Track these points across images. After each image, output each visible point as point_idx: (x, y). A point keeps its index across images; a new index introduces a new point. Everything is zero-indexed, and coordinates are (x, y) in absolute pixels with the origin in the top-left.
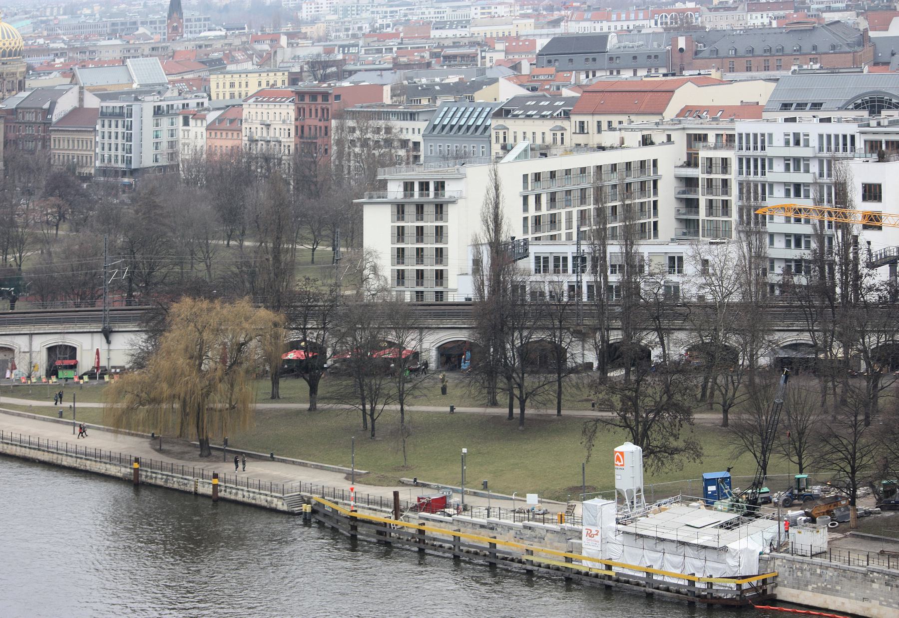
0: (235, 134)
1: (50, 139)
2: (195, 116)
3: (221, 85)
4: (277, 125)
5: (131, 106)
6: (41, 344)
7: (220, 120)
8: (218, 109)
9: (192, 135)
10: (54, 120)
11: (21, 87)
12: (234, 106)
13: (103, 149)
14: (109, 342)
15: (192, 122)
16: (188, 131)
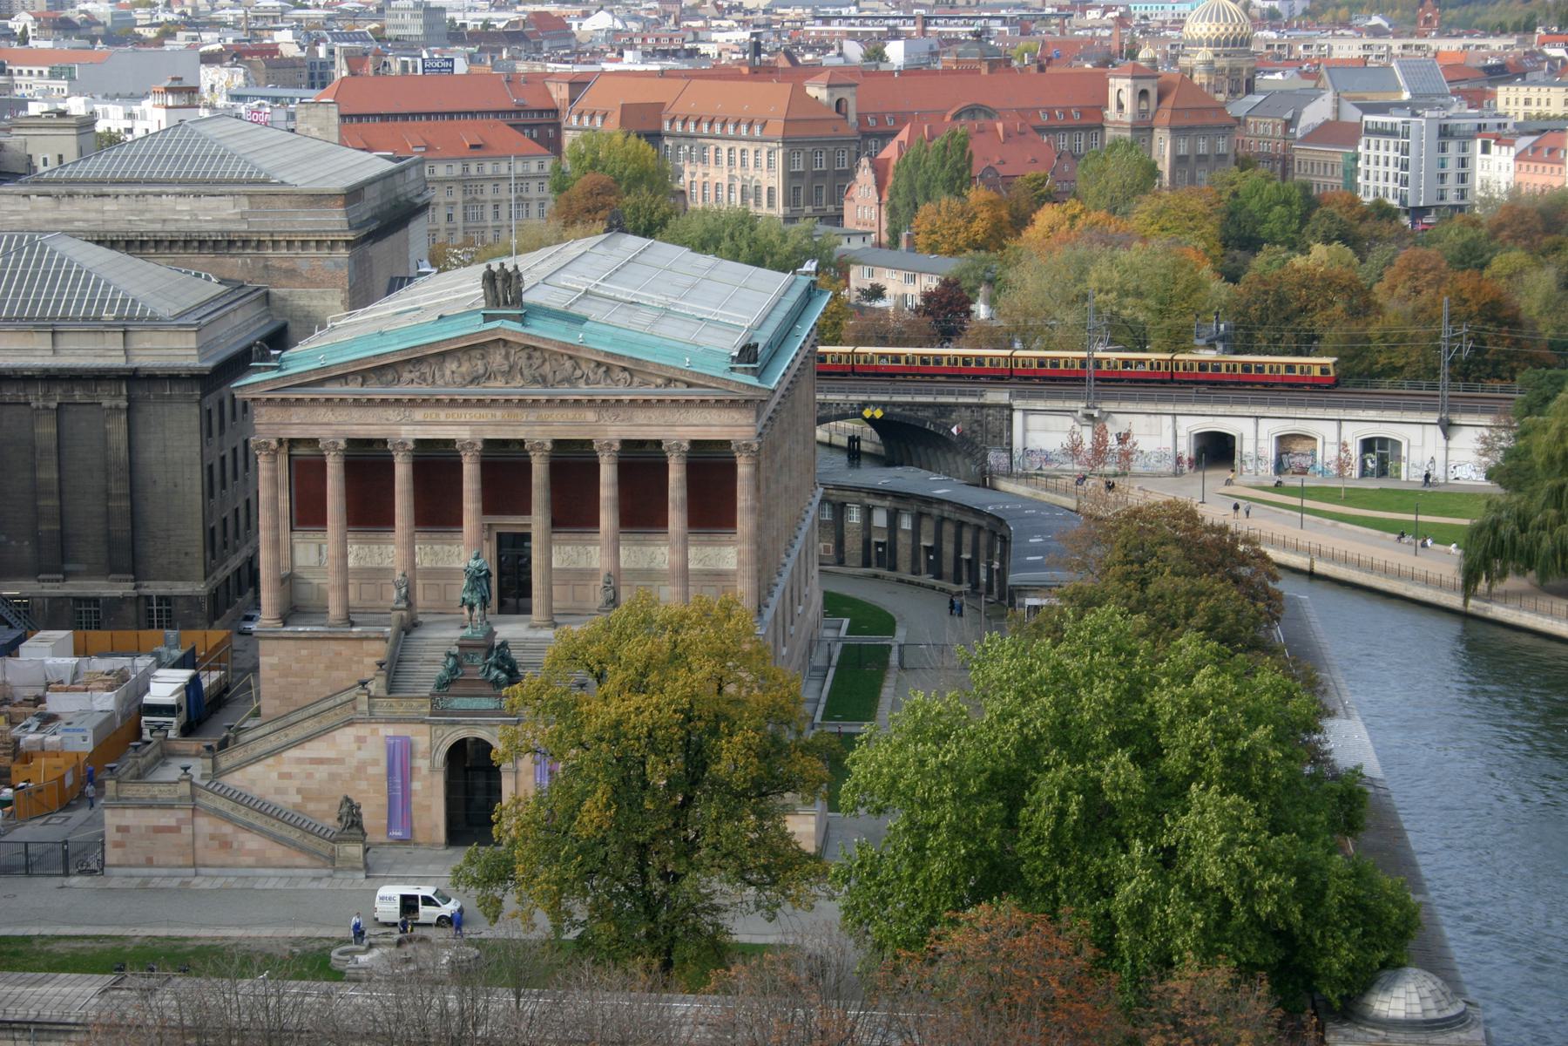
0: (1556, 167)
1: (1293, 160)
2: (1499, 141)
3: (1512, 101)
5: (1408, 122)
6: (1354, 434)
7: (1535, 148)
8: (1530, 134)
9: (1494, 165)
10: (1299, 135)
11: (1250, 89)
12: (1552, 131)
13: (1367, 178)
14: (1447, 437)
15: (1494, 149)
16: (1489, 160)
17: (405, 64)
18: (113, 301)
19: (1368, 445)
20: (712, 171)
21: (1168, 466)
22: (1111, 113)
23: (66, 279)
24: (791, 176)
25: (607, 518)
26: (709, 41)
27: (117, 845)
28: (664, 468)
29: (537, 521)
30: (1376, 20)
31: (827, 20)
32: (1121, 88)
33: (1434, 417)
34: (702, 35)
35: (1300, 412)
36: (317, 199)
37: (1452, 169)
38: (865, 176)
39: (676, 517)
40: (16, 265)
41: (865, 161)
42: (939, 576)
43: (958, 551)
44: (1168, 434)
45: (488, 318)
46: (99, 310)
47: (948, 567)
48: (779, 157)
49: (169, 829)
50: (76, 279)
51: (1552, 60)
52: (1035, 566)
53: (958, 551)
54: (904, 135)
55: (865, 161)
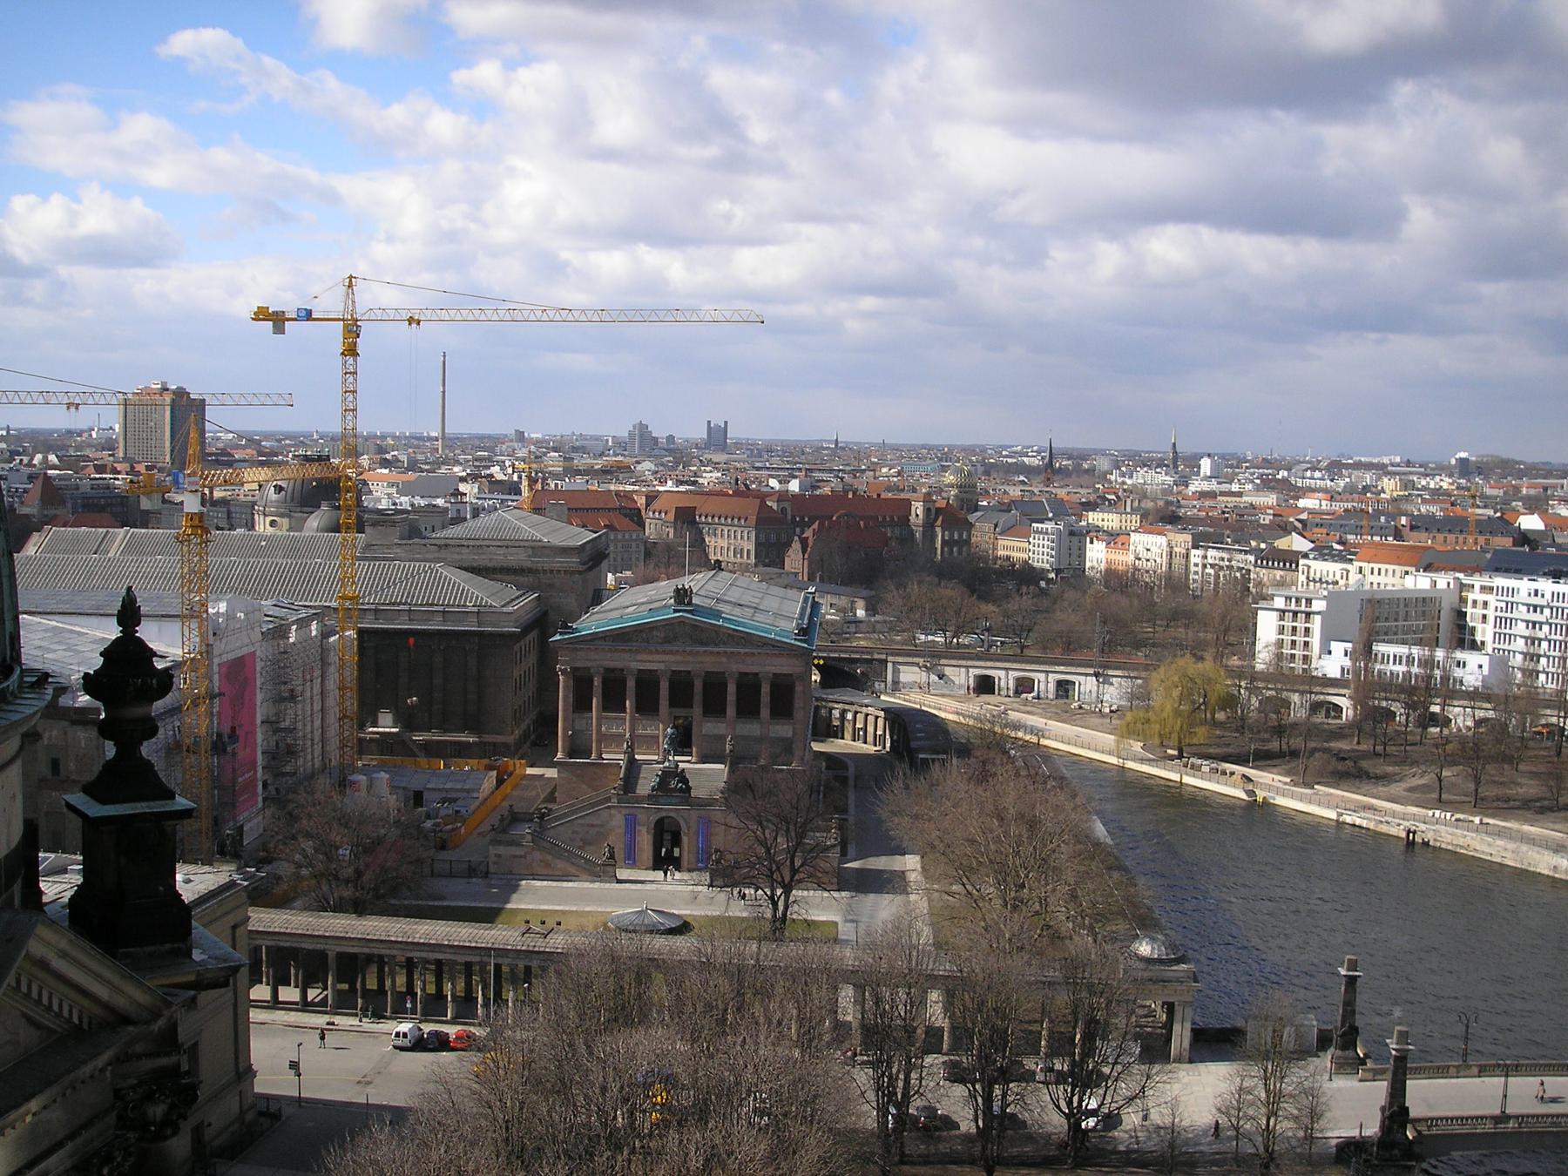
4: (1154, 549)
17: (556, 485)
18: (471, 598)
19: (1060, 684)
20: (719, 540)
21: (963, 691)
22: (912, 518)
23: (449, 585)
24: (758, 544)
25: (731, 711)
26: (702, 477)
27: (495, 863)
28: (725, 685)
29: (697, 710)
30: (1022, 478)
31: (758, 469)
32: (918, 508)
33: (1091, 671)
34: (699, 474)
35: (1028, 667)
36: (565, 551)
37: (1075, 552)
38: (796, 545)
39: (765, 712)
40: (424, 579)
41: (796, 538)
42: (865, 742)
43: (876, 730)
44: (963, 675)
45: (675, 611)
46: (465, 602)
47: (870, 738)
48: (753, 535)
49: (521, 856)
50: (453, 587)
51: (1109, 501)
52: (921, 739)
53: (876, 730)
54: (816, 526)
55: (796, 538)
